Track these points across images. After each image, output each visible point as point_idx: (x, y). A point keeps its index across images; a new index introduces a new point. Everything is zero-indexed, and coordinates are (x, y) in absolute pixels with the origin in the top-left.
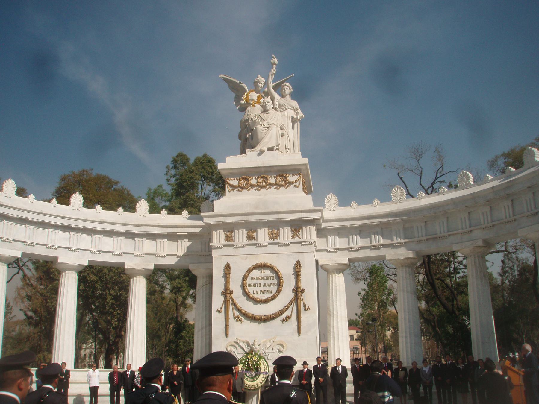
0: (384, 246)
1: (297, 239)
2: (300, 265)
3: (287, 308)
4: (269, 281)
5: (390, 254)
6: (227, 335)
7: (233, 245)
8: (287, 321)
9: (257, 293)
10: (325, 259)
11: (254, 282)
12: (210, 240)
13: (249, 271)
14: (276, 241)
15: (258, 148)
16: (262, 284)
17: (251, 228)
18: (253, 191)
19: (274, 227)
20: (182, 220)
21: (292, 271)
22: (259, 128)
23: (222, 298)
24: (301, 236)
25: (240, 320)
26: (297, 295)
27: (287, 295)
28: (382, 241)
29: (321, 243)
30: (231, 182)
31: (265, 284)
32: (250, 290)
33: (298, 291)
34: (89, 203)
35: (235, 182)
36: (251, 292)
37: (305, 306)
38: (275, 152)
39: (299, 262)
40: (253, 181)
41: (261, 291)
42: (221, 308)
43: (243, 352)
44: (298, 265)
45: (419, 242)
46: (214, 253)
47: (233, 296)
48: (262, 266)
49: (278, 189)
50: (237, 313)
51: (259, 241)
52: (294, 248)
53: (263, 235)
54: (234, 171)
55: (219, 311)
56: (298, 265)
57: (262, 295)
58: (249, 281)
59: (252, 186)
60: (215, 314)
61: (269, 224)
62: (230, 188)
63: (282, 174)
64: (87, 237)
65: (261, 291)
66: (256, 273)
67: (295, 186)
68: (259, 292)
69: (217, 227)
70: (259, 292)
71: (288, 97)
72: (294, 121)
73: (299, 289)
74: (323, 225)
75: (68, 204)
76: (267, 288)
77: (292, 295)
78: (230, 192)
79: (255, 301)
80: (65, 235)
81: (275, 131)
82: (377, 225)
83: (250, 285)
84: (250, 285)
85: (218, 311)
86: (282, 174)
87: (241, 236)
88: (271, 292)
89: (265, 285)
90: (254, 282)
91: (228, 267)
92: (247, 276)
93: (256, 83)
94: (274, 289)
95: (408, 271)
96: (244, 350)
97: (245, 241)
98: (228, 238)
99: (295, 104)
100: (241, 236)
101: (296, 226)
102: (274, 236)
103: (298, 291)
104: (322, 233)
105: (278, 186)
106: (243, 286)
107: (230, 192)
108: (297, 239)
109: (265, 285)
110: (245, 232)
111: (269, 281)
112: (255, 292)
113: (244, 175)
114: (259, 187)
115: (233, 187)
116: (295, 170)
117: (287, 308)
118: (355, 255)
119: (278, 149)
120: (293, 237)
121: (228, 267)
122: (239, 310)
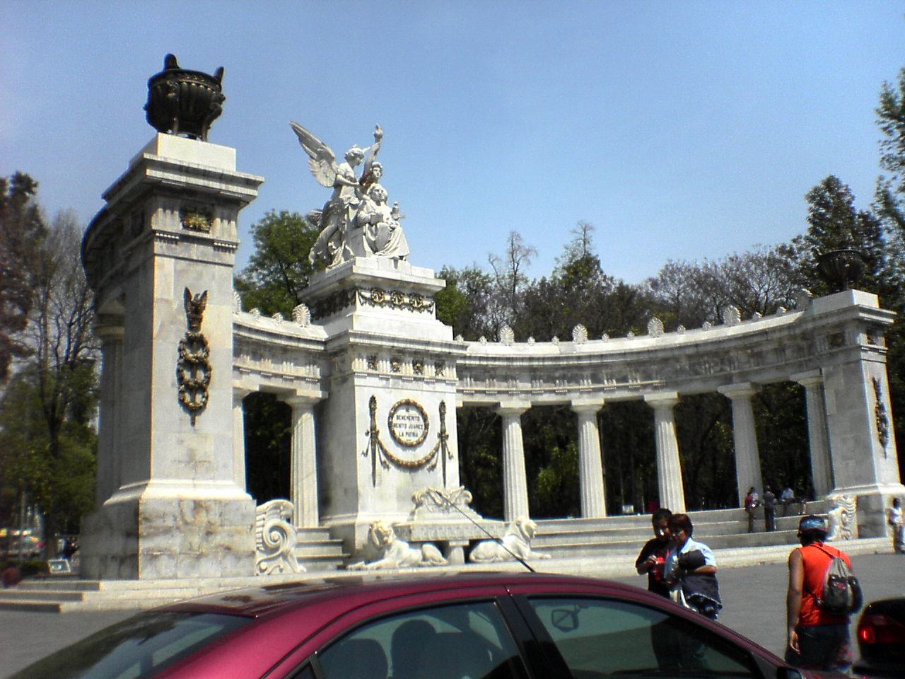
1: (440, 377)
2: (445, 406)
4: (415, 422)
6: (374, 484)
8: (433, 470)
13: (395, 409)
14: (420, 375)
16: (408, 425)
18: (387, 308)
19: (419, 359)
23: (368, 438)
24: (444, 373)
25: (388, 467)
26: (442, 441)
27: (433, 440)
30: (363, 293)
32: (397, 431)
33: (443, 436)
35: (368, 295)
42: (367, 451)
43: (433, 503)
46: (357, 381)
47: (380, 437)
48: (408, 404)
50: (384, 458)
55: (366, 454)
58: (395, 421)
60: (360, 458)
62: (362, 300)
65: (407, 433)
66: (402, 412)
67: (429, 311)
68: (405, 434)
70: (405, 434)
73: (443, 435)
76: (413, 430)
77: (437, 440)
78: (362, 304)
84: (395, 425)
85: (363, 453)
88: (417, 436)
89: (411, 427)
91: (373, 400)
92: (393, 414)
94: (420, 432)
96: (434, 501)
100: (384, 366)
102: (418, 370)
103: (443, 436)
106: (390, 425)
107: (362, 304)
108: (440, 377)
109: (411, 427)
111: (415, 422)
121: (373, 400)
122: (386, 453)
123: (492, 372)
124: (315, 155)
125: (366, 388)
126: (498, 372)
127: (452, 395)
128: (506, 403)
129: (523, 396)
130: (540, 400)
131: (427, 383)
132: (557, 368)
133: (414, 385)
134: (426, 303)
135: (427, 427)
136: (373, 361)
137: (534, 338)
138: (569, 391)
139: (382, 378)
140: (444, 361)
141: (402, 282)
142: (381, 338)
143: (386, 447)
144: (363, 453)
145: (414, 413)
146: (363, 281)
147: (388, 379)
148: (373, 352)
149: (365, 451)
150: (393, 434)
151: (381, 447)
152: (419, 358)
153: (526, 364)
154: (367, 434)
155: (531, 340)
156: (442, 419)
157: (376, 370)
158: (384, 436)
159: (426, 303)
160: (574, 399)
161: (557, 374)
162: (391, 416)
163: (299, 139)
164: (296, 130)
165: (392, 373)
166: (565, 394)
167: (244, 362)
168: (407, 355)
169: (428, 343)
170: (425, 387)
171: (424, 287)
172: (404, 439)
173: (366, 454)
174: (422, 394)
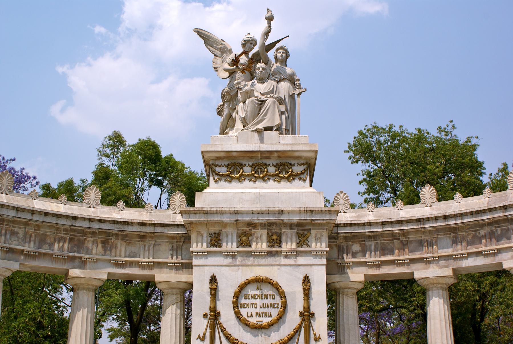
2: (309, 281)
7: (222, 252)
9: (252, 316)
11: (247, 301)
16: (259, 304)
23: (205, 322)
24: (309, 244)
26: (303, 320)
30: (218, 169)
31: (263, 304)
32: (244, 312)
36: (245, 316)
37: (315, 335)
38: (274, 134)
39: (308, 277)
41: (257, 313)
42: (204, 335)
44: (306, 280)
46: (195, 262)
48: (259, 281)
49: (279, 182)
52: (301, 260)
54: (222, 155)
55: (202, 339)
56: (306, 280)
57: (258, 319)
62: (216, 178)
65: (257, 313)
67: (300, 179)
68: (254, 314)
70: (254, 314)
77: (298, 320)
83: (243, 306)
85: (199, 337)
88: (271, 316)
90: (247, 301)
94: (275, 312)
95: (441, 293)
102: (275, 240)
107: (216, 181)
108: (304, 249)
112: (249, 315)
119: (276, 130)
120: (299, 245)
123: (403, 238)
124: (218, 53)
125: (207, 268)
126: (411, 237)
127: (319, 267)
128: (420, 273)
129: (442, 263)
130: (464, 265)
131: (287, 257)
132: (481, 225)
133: (270, 260)
134: (297, 169)
135: (285, 306)
136: (216, 240)
137: (461, 193)
138: (499, 251)
139: (227, 255)
140: (310, 229)
141: (262, 152)
142: (221, 213)
143: (229, 330)
144: (199, 337)
146: (219, 158)
147: (234, 257)
148: (217, 229)
149: (201, 336)
151: (223, 330)
152: (275, 229)
153: (441, 224)
154: (205, 316)
155: (458, 196)
157: (220, 246)
160: (505, 260)
161: (482, 233)
162: (237, 296)
163: (205, 42)
164: (200, 33)
165: (241, 249)
166: (495, 254)
167: (88, 251)
168: (259, 228)
169: (282, 212)
170: (284, 261)
171: (289, 154)
172: (253, 320)
173: (202, 339)
174: (278, 269)
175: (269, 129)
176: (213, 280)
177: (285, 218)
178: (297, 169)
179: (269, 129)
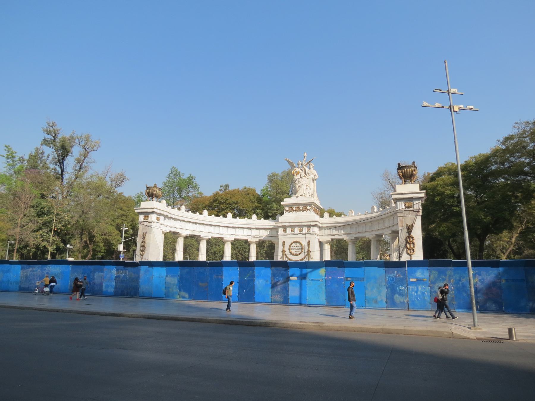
0: (343, 234)
3: (304, 258)
5: (345, 238)
10: (322, 239)
12: (278, 232)
13: (292, 244)
15: (296, 195)
17: (293, 227)
19: (301, 227)
20: (269, 223)
21: (307, 244)
22: (297, 186)
23: (282, 254)
28: (343, 232)
29: (321, 233)
32: (292, 251)
33: (309, 252)
34: (234, 216)
35: (287, 209)
40: (294, 209)
44: (309, 242)
45: (356, 233)
51: (295, 233)
52: (307, 235)
53: (297, 230)
56: (309, 242)
58: (291, 247)
59: (294, 211)
61: (298, 226)
63: (304, 207)
64: (233, 230)
66: (294, 245)
69: (280, 227)
71: (312, 169)
72: (313, 180)
74: (320, 225)
75: (226, 217)
77: (306, 254)
79: (293, 255)
80: (226, 229)
81: (304, 187)
82: (342, 226)
86: (304, 207)
87: (289, 230)
91: (284, 242)
93: (298, 164)
94: (300, 251)
97: (290, 232)
98: (284, 231)
99: (315, 172)
100: (289, 230)
101: (309, 227)
103: (309, 252)
104: (320, 228)
105: (303, 211)
106: (289, 249)
110: (290, 229)
113: (291, 206)
114: (296, 211)
115: (287, 211)
116: (310, 204)
117: (304, 258)
118: (333, 237)
122: (288, 258)
143: (288, 256)
145: (298, 244)
150: (290, 252)
156: (309, 247)
158: (287, 253)
159: (309, 208)
162: (290, 246)
164: (287, 161)
172: (294, 253)
175: (302, 195)
176: (284, 242)
177: (303, 224)
178: (309, 208)
179: (302, 195)
